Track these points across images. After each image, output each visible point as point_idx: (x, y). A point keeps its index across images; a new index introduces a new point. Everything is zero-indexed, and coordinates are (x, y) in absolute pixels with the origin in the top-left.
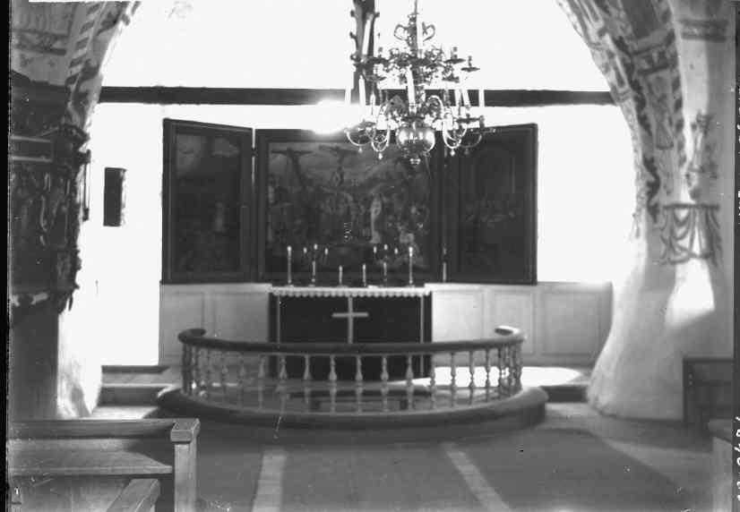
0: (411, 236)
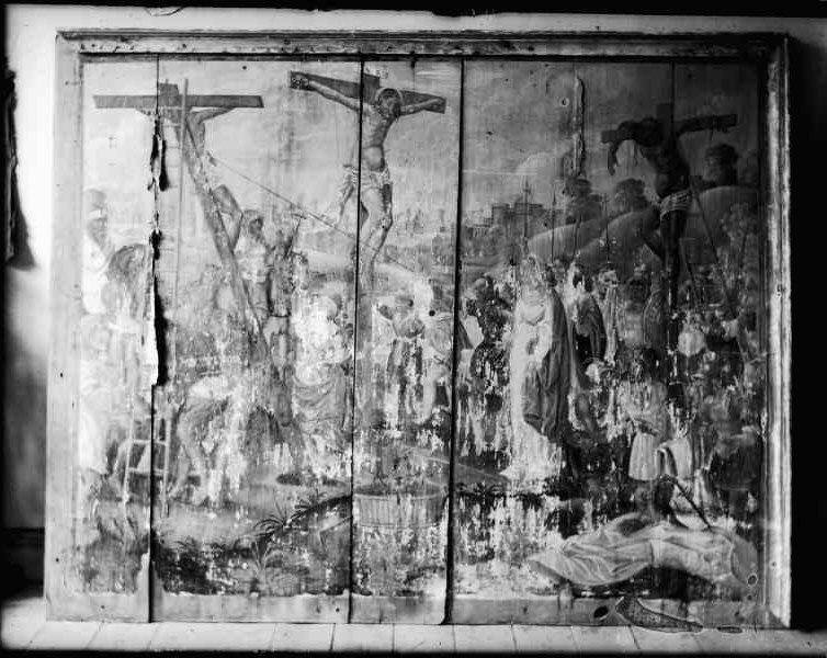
0: (681, 448)
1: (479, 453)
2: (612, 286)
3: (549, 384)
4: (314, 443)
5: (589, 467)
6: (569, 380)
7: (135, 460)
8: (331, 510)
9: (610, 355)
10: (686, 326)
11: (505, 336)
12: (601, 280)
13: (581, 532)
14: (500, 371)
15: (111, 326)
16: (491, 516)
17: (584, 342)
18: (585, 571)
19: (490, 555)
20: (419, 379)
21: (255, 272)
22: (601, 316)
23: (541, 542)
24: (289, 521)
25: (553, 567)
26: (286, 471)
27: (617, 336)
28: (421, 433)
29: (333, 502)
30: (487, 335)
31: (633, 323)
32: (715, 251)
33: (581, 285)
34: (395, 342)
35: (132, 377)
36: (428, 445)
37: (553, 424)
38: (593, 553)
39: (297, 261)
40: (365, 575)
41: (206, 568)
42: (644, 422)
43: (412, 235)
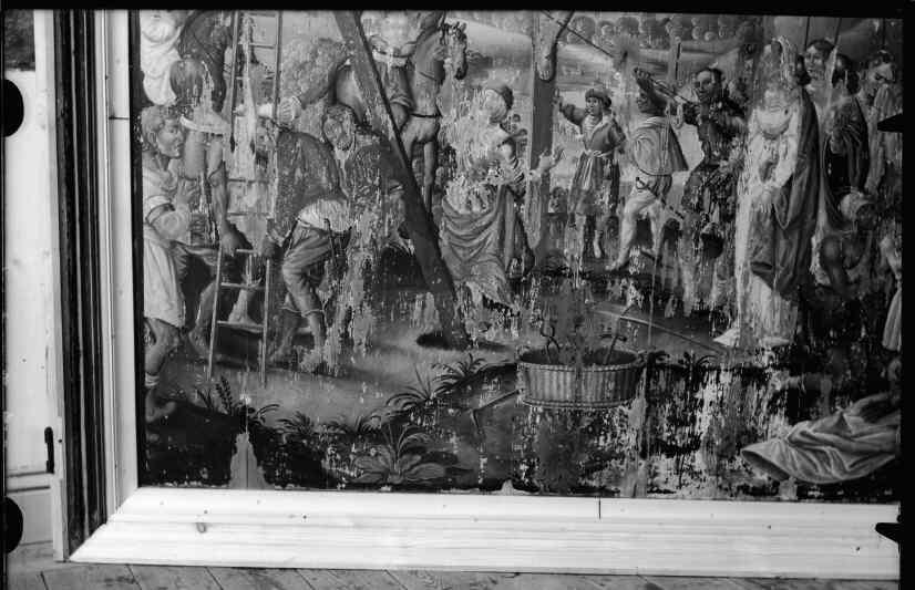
1: (688, 311)
2: (886, 86)
3: (788, 221)
4: (468, 293)
5: (831, 333)
6: (815, 216)
7: (224, 311)
8: (489, 383)
9: (872, 181)
11: (735, 154)
12: (871, 77)
13: (813, 417)
14: (723, 203)
15: (185, 122)
16: (698, 396)
18: (815, 466)
19: (695, 443)
20: (613, 210)
21: (390, 51)
22: (866, 128)
23: (761, 428)
24: (433, 395)
25: (774, 460)
26: (428, 329)
27: (884, 157)
28: (613, 283)
29: (493, 372)
30: (709, 153)
33: (843, 84)
34: (584, 157)
35: (217, 194)
36: (623, 299)
38: (827, 443)
39: (451, 39)
40: (532, 466)
41: (322, 455)
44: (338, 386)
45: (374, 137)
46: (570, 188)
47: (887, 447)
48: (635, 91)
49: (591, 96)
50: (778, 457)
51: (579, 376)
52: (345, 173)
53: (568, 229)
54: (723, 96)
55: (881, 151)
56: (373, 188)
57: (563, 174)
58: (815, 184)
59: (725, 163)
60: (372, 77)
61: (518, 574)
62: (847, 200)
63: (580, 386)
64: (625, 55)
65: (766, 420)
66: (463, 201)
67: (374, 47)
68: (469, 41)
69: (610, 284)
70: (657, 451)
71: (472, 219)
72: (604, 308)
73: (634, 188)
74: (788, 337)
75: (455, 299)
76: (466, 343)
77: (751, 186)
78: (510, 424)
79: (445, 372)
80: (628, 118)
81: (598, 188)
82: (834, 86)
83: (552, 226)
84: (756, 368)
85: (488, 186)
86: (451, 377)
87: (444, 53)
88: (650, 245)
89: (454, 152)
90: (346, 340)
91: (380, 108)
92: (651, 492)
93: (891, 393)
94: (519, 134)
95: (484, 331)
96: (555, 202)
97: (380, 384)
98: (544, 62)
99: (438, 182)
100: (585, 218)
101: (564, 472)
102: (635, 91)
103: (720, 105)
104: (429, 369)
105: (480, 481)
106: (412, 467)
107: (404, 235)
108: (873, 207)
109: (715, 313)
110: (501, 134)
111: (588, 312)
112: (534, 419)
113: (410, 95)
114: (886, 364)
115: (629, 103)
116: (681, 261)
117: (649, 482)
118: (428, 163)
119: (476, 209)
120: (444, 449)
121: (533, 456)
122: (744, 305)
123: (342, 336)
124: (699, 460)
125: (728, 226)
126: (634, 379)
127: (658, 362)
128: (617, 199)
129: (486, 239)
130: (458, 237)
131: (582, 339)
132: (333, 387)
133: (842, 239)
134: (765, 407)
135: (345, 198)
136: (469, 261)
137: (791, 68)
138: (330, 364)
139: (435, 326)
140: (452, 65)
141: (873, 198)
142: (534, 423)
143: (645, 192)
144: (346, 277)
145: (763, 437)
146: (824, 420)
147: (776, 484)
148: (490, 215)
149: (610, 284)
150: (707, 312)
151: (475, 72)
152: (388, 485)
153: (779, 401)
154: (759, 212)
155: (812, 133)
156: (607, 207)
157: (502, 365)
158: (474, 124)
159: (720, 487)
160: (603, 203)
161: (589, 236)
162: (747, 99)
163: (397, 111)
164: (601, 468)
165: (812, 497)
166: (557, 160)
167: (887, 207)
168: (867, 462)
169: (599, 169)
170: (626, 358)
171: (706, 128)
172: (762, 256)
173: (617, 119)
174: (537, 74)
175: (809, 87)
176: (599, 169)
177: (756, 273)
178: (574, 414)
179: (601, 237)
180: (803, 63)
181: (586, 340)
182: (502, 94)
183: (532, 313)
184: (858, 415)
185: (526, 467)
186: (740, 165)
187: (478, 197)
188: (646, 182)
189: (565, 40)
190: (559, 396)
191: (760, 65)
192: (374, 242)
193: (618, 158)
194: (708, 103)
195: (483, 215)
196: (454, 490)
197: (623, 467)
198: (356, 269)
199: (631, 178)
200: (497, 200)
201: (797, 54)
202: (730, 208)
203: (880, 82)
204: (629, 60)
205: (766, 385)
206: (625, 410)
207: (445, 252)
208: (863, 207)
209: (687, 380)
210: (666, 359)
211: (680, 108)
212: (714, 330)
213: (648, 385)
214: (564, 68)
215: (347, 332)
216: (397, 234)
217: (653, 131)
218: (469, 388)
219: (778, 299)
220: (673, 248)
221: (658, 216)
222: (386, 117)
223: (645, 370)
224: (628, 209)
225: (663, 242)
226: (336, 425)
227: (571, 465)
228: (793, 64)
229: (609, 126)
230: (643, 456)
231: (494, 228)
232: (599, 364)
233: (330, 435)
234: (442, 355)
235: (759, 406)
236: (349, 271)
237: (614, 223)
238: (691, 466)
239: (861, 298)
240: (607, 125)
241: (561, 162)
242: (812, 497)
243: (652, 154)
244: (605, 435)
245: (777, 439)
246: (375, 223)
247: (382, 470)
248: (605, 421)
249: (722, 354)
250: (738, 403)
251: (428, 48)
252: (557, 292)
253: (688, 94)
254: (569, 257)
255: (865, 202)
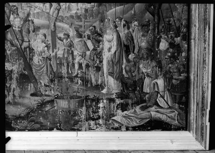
0: (161, 82)
1: (94, 85)
2: (137, 27)
3: (116, 62)
4: (41, 83)
5: (130, 89)
6: (123, 60)
8: (48, 104)
10: (162, 40)
11: (101, 46)
12: (133, 25)
13: (128, 110)
14: (99, 58)
16: (99, 106)
17: (127, 47)
18: (130, 122)
19: (99, 118)
20: (73, 61)
23: (115, 113)
24: (35, 108)
26: (32, 92)
27: (138, 45)
29: (49, 102)
30: (94, 46)
31: (144, 40)
32: (172, 14)
33: (126, 28)
34: (64, 49)
36: (77, 83)
37: (118, 75)
38: (132, 116)
39: (31, 23)
40: (60, 124)
41: (11, 123)
42: (148, 73)
43: (68, 12)
44: (13, 107)
45: (15, 47)
46: (62, 57)
47: (148, 117)
48: (75, 32)
49: (65, 34)
50: (120, 120)
51: (69, 102)
52: (10, 56)
53: (63, 67)
54: (96, 32)
55: (137, 43)
56: (16, 59)
57: (60, 53)
58: (121, 52)
59: (99, 49)
60: (13, 33)
61: (55, 151)
62: (130, 56)
63: (69, 104)
64: (72, 24)
65: (116, 111)
66: (37, 61)
67: (13, 26)
68: (35, 23)
69: (74, 79)
70: (90, 120)
71: (40, 66)
72: (73, 85)
73: (77, 56)
74: (119, 90)
75: (38, 85)
76: (41, 95)
77: (106, 53)
78: (54, 114)
79: (37, 102)
80: (74, 39)
81: (69, 56)
82: (124, 28)
83: (59, 66)
84: (112, 98)
85: (43, 57)
86: (39, 103)
87: (29, 27)
88: (83, 70)
89: (34, 50)
90: (14, 96)
91: (16, 40)
92: (90, 130)
93: (147, 103)
94: (48, 45)
95: (45, 92)
96: (59, 60)
97: (23, 106)
98: (53, 27)
99: (31, 57)
100: (66, 64)
101: (68, 125)
102: (75, 32)
103: (96, 35)
104: (33, 102)
105: (49, 128)
106: (32, 125)
107: (25, 70)
108: (137, 57)
109: (101, 85)
110: (45, 45)
111: (70, 86)
112: (60, 113)
113: (22, 37)
114: (145, 96)
115: (74, 35)
116: (90, 73)
117: (89, 127)
118: (28, 53)
119: (40, 63)
120: (39, 121)
121: (61, 122)
122: (107, 83)
123: (13, 95)
124: (101, 121)
125: (101, 64)
126: (82, 102)
127: (88, 98)
128: (73, 59)
129: (43, 70)
130: (37, 70)
131: (69, 93)
132: (12, 107)
133: (130, 65)
134: (115, 108)
135: (10, 62)
136: (40, 75)
137: (112, 25)
138: (11, 101)
139: (34, 91)
140: (31, 29)
141: (137, 55)
142: (60, 114)
143: (80, 56)
144: (12, 81)
145: (116, 115)
146: (131, 111)
147: (120, 127)
148: (44, 64)
149: (74, 79)
150: (98, 85)
151: (36, 31)
152: (27, 130)
153: (119, 106)
154: (109, 60)
155: (120, 40)
156: (71, 61)
157: (50, 100)
158: (38, 43)
159: (107, 128)
160: (70, 60)
161: (68, 68)
162: (103, 33)
163: (20, 41)
164: (77, 124)
165: (130, 130)
166: (58, 50)
167: (141, 57)
168: (143, 121)
169: (68, 52)
170: (80, 97)
171: (93, 40)
172: (110, 71)
173: (71, 39)
174: (51, 30)
175: (118, 29)
176: (68, 52)
177: (109, 75)
178: (69, 111)
179: (71, 68)
180: (115, 23)
181: (70, 93)
182: (43, 35)
183: (56, 87)
184: (139, 109)
185: (59, 125)
186: (103, 49)
187: (41, 60)
188: (80, 54)
189: (57, 21)
190: (65, 107)
191: (105, 24)
192: (18, 72)
193: (72, 49)
194: (93, 34)
195: (43, 64)
196: (42, 131)
197: (82, 124)
198: (14, 79)
199: (76, 54)
200: (45, 61)
201: (114, 21)
202: (101, 59)
203: (135, 26)
204: (73, 25)
205: (115, 102)
206: (81, 110)
207: (34, 74)
208: (134, 57)
209: (95, 102)
210: (90, 97)
211: (86, 36)
212: (101, 89)
213: (86, 104)
214: (57, 28)
215: (14, 94)
216: (23, 70)
217: (80, 42)
218: (43, 106)
219: (116, 81)
220: (88, 70)
221: (84, 63)
222: (17, 42)
223: (85, 100)
224: (76, 61)
225: (86, 69)
226: (14, 116)
227: (70, 124)
228: (113, 23)
229: (70, 42)
230: (87, 121)
231: (45, 67)
232: (73, 99)
233: (12, 118)
234: (36, 98)
235: (114, 108)
236: (13, 80)
237: (73, 65)
238: (99, 123)
239: (136, 80)
240: (69, 41)
241: (59, 51)
242: (130, 130)
243: (81, 48)
244: (77, 116)
245: (119, 116)
246: (18, 68)
247: (25, 126)
248: (77, 113)
249: (103, 95)
250: (109, 107)
251: (25, 26)
252: (62, 82)
253: (88, 32)
254: (64, 73)
255: (135, 56)
